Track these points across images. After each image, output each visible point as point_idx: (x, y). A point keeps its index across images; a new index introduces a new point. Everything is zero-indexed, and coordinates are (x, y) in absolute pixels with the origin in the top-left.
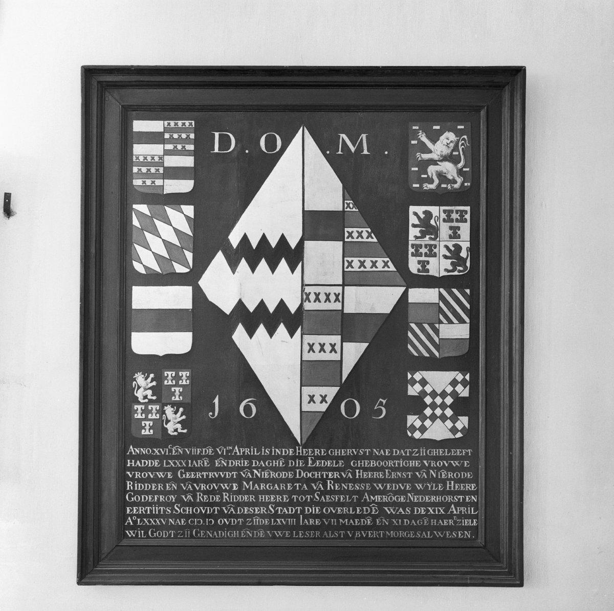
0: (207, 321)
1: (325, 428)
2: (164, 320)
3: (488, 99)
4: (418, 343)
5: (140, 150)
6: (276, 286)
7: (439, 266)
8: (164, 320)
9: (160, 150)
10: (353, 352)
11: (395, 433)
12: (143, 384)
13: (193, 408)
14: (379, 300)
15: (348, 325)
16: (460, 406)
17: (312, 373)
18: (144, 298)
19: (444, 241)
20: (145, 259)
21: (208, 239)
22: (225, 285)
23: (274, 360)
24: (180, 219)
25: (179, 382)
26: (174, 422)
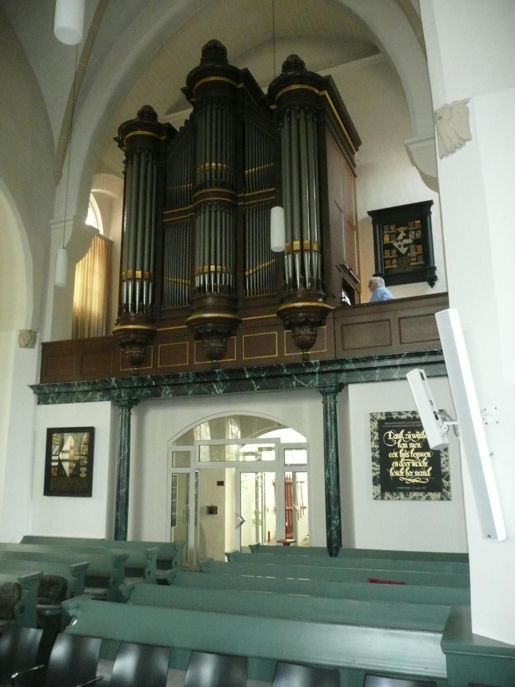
0: (60, 461)
1: (71, 475)
2: (55, 461)
3: (91, 431)
4: (81, 464)
5: (54, 438)
6: (66, 456)
7: (84, 453)
8: (55, 461)
9: (56, 437)
10: (74, 465)
11: (79, 476)
12: (53, 469)
13: (58, 472)
14: (77, 458)
15: (74, 461)
16: (86, 472)
17: (70, 468)
18: (54, 458)
19: (85, 450)
20: (54, 453)
21: (60, 450)
22: (62, 456)
23: (66, 465)
24: (57, 447)
25: (56, 469)
26: (56, 475)
